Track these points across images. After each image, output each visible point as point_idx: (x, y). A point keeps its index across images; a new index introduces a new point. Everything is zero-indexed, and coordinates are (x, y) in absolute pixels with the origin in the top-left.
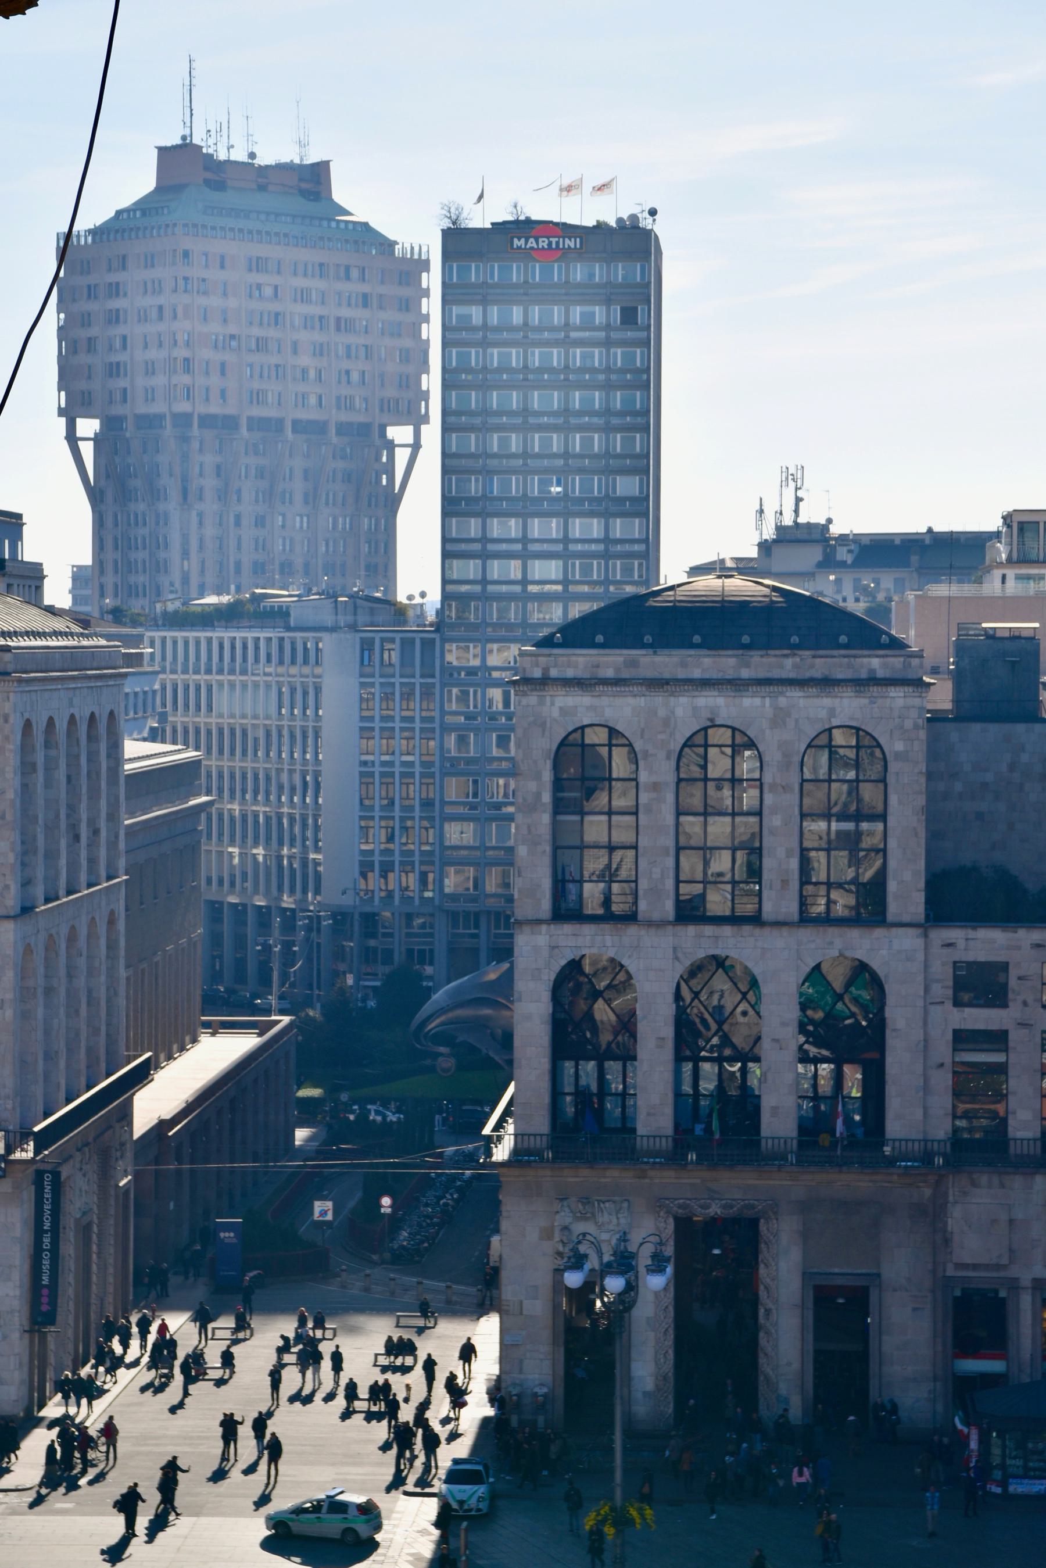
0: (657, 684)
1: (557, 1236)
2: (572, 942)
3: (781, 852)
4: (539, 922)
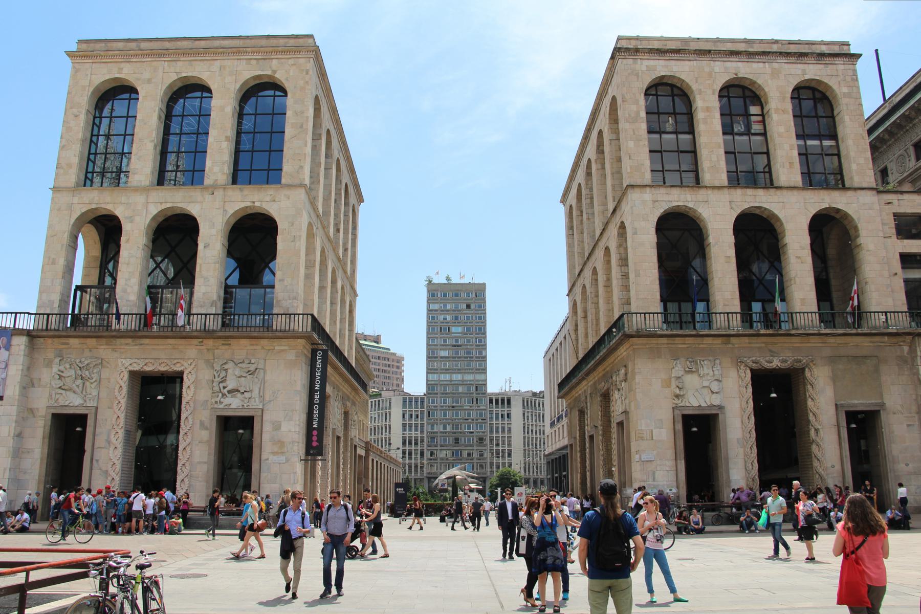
1: (674, 383)
2: (666, 198)
3: (786, 147)
4: (645, 186)
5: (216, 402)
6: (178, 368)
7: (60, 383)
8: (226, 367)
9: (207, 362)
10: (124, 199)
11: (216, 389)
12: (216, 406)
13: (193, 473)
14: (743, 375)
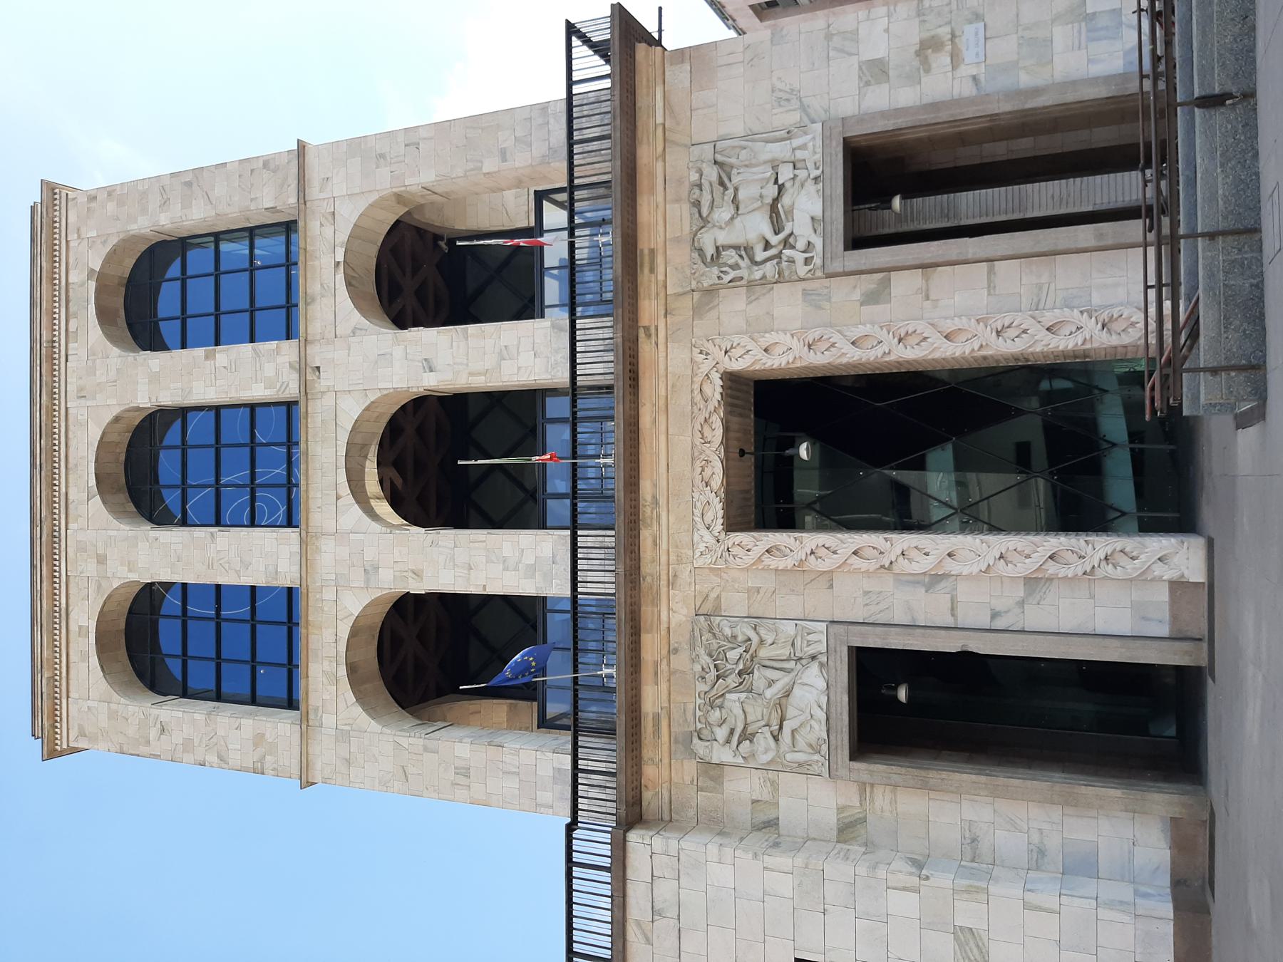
5: (807, 261)
6: (715, 390)
7: (764, 740)
8: (710, 251)
9: (698, 311)
11: (769, 269)
12: (818, 261)
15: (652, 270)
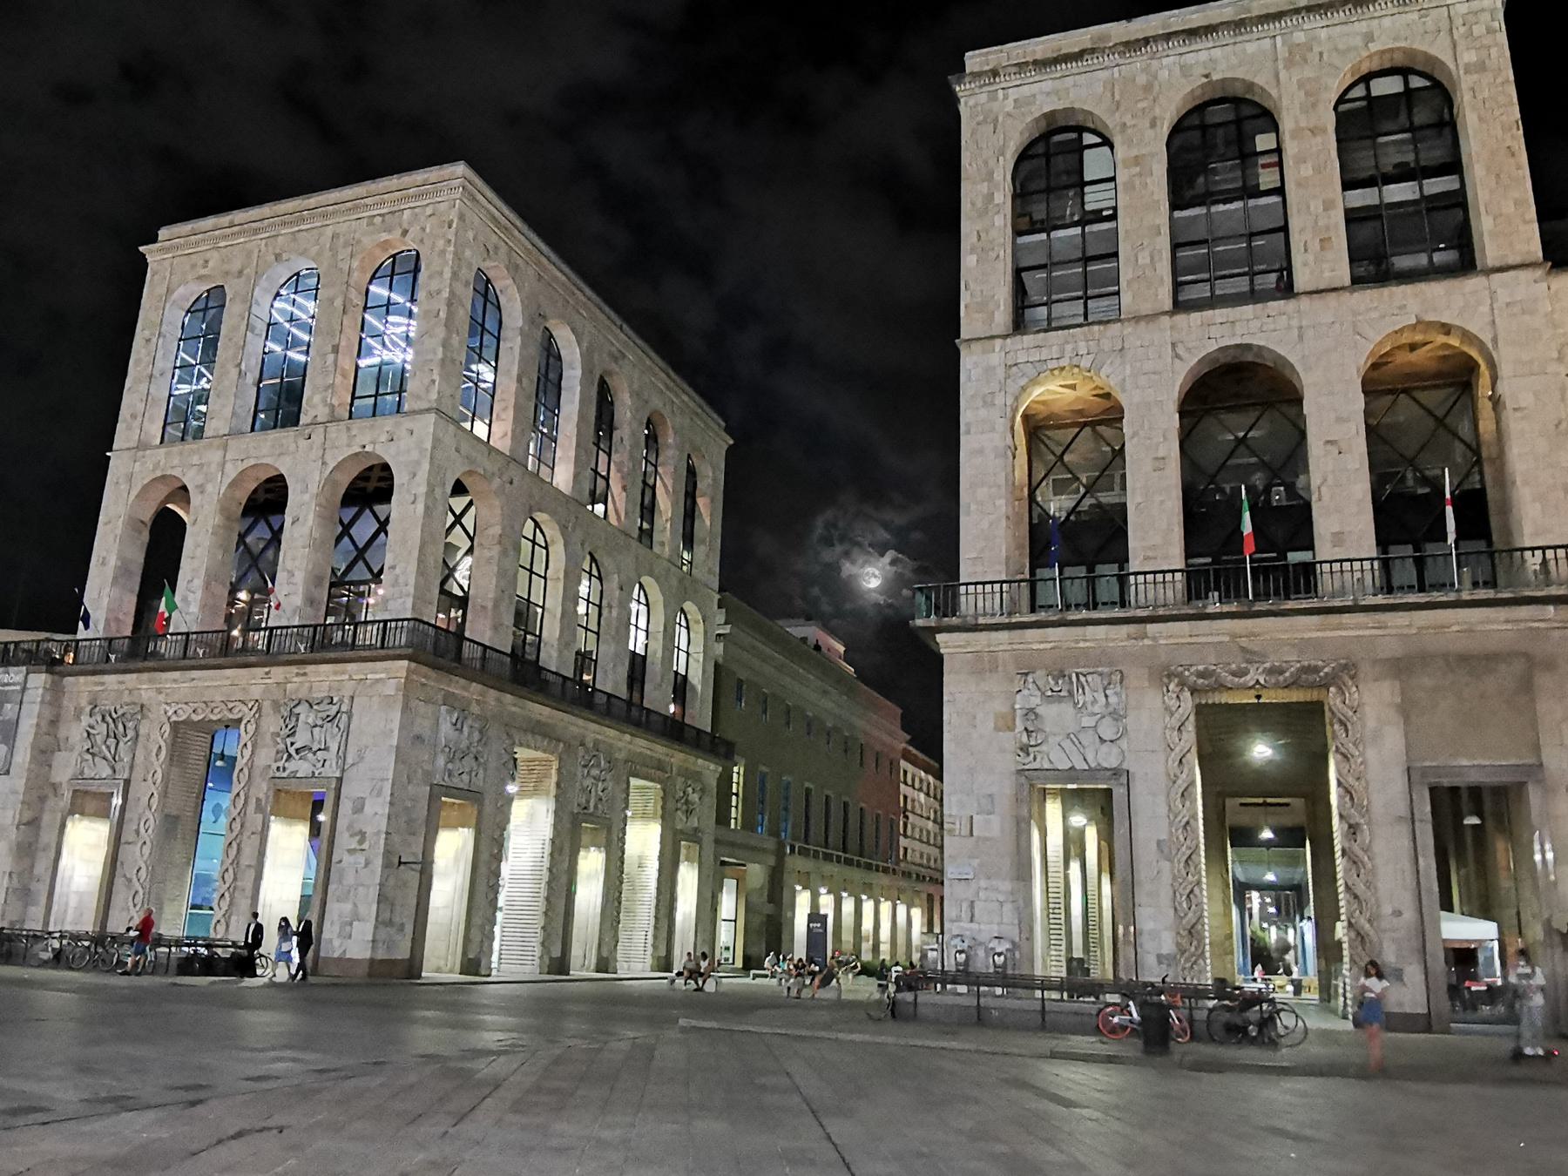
0: (1132, 46)
1: (1020, 726)
3: (1316, 206)
8: (296, 711)
10: (195, 460)
11: (282, 746)
13: (239, 883)
14: (1173, 703)
15: (298, 675)
